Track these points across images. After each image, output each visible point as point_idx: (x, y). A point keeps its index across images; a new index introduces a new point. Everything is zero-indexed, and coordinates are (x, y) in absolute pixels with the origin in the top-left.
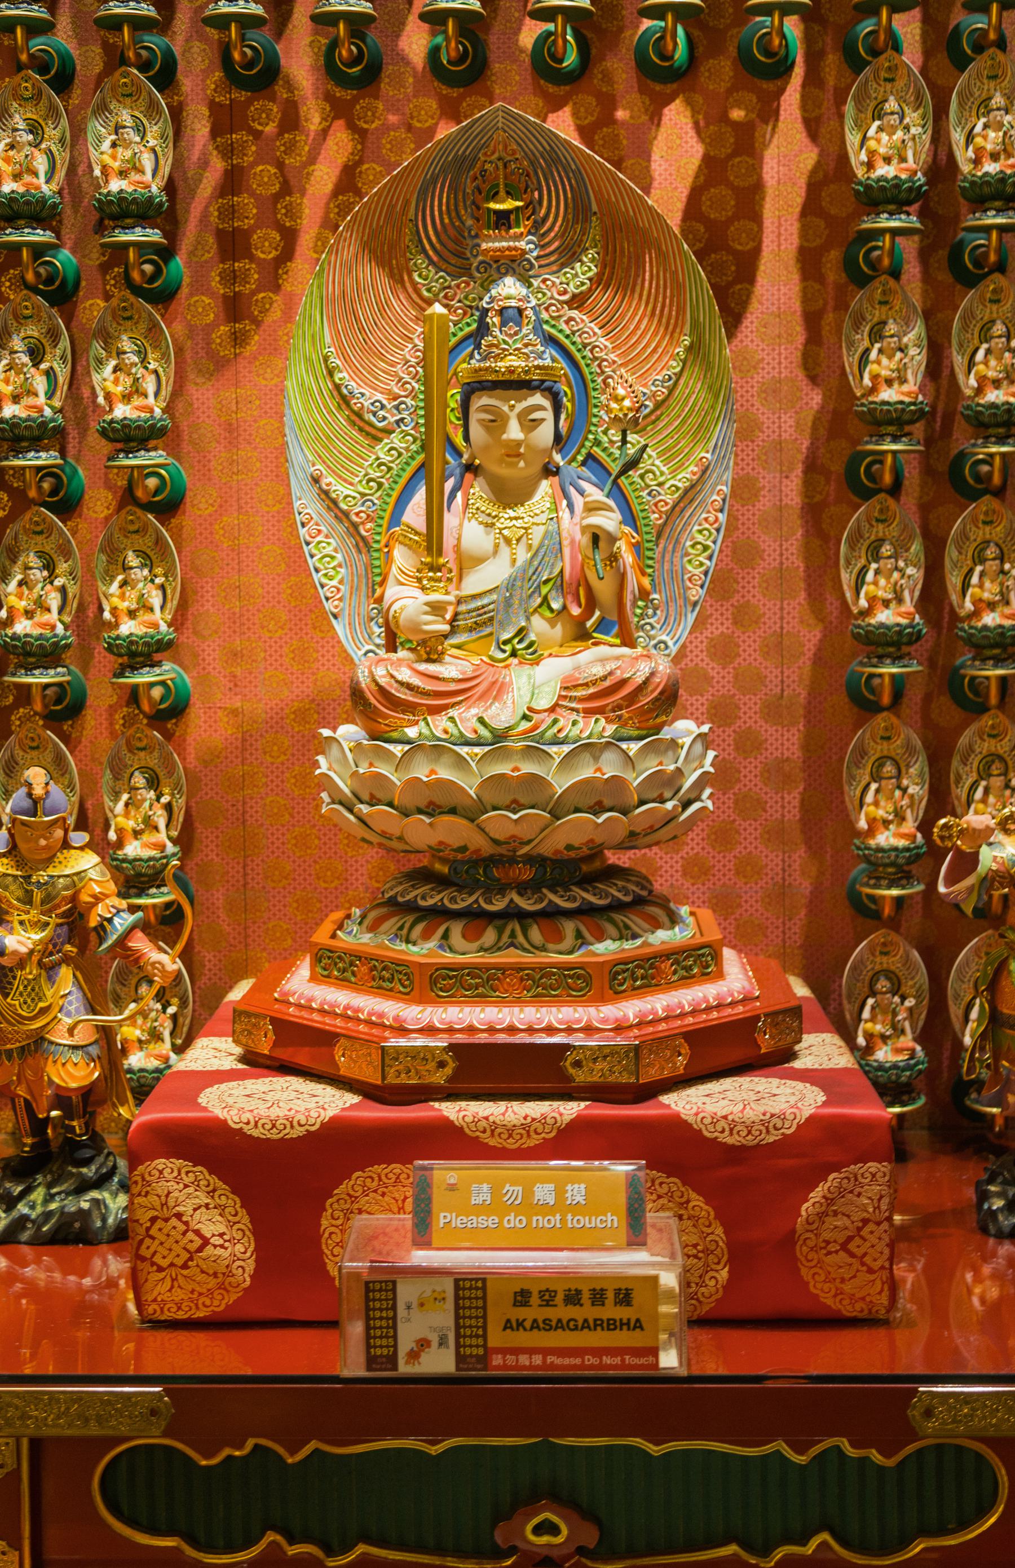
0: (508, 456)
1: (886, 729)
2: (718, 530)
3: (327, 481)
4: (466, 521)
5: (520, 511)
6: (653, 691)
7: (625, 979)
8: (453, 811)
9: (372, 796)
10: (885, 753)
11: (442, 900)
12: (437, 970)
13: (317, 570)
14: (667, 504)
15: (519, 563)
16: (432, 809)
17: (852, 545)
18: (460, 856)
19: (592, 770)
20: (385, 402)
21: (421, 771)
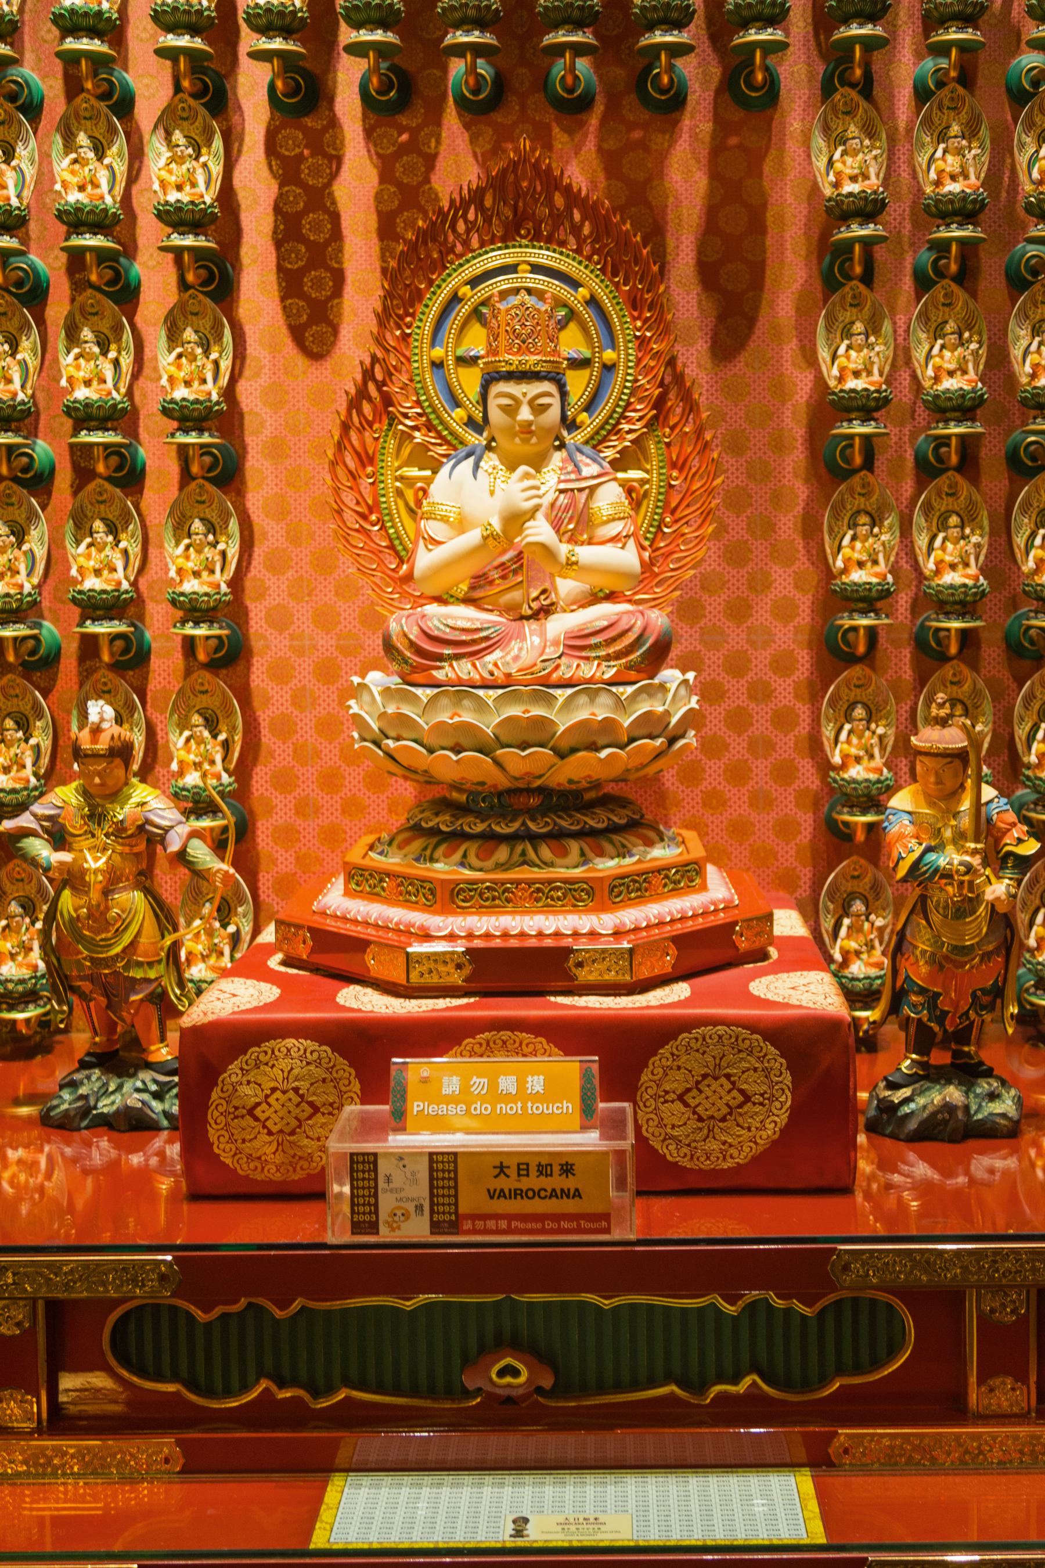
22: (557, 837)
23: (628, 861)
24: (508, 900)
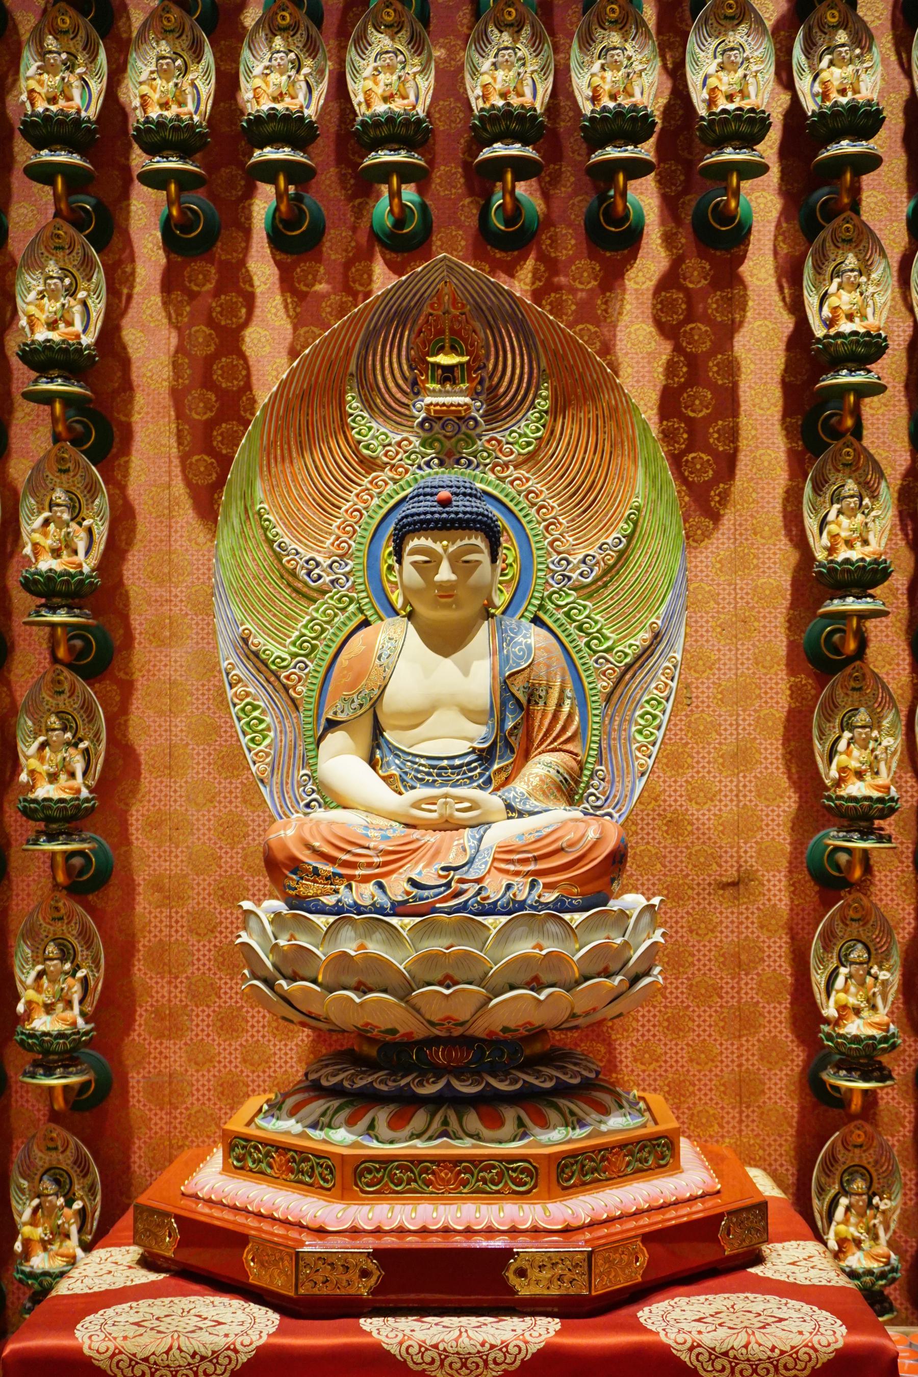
7: (573, 1173)
22: (489, 1106)
23: (579, 1133)
24: (428, 1183)
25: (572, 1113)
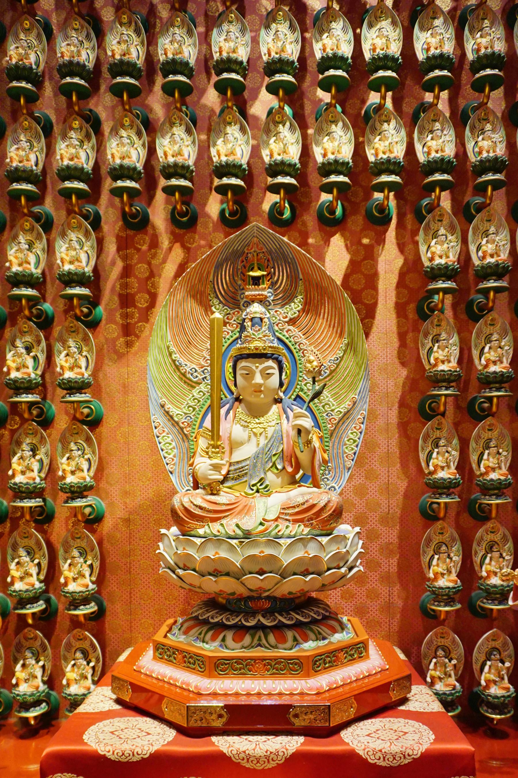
0: (255, 392)
1: (441, 529)
2: (361, 433)
3: (168, 407)
4: (234, 425)
5: (262, 420)
6: (329, 511)
8: (228, 574)
9: (185, 565)
10: (441, 540)
11: (222, 619)
12: (219, 660)
13: (162, 450)
14: (335, 420)
15: (261, 445)
16: (216, 573)
17: (425, 441)
18: (231, 597)
19: (303, 553)
20: (197, 369)
21: (211, 553)
22: (279, 629)
23: (321, 643)
25: (320, 633)
